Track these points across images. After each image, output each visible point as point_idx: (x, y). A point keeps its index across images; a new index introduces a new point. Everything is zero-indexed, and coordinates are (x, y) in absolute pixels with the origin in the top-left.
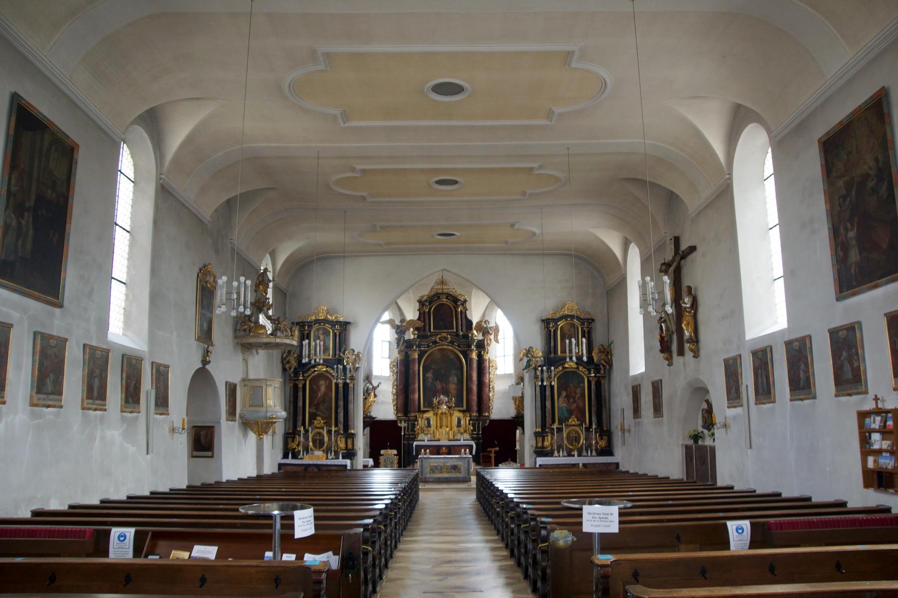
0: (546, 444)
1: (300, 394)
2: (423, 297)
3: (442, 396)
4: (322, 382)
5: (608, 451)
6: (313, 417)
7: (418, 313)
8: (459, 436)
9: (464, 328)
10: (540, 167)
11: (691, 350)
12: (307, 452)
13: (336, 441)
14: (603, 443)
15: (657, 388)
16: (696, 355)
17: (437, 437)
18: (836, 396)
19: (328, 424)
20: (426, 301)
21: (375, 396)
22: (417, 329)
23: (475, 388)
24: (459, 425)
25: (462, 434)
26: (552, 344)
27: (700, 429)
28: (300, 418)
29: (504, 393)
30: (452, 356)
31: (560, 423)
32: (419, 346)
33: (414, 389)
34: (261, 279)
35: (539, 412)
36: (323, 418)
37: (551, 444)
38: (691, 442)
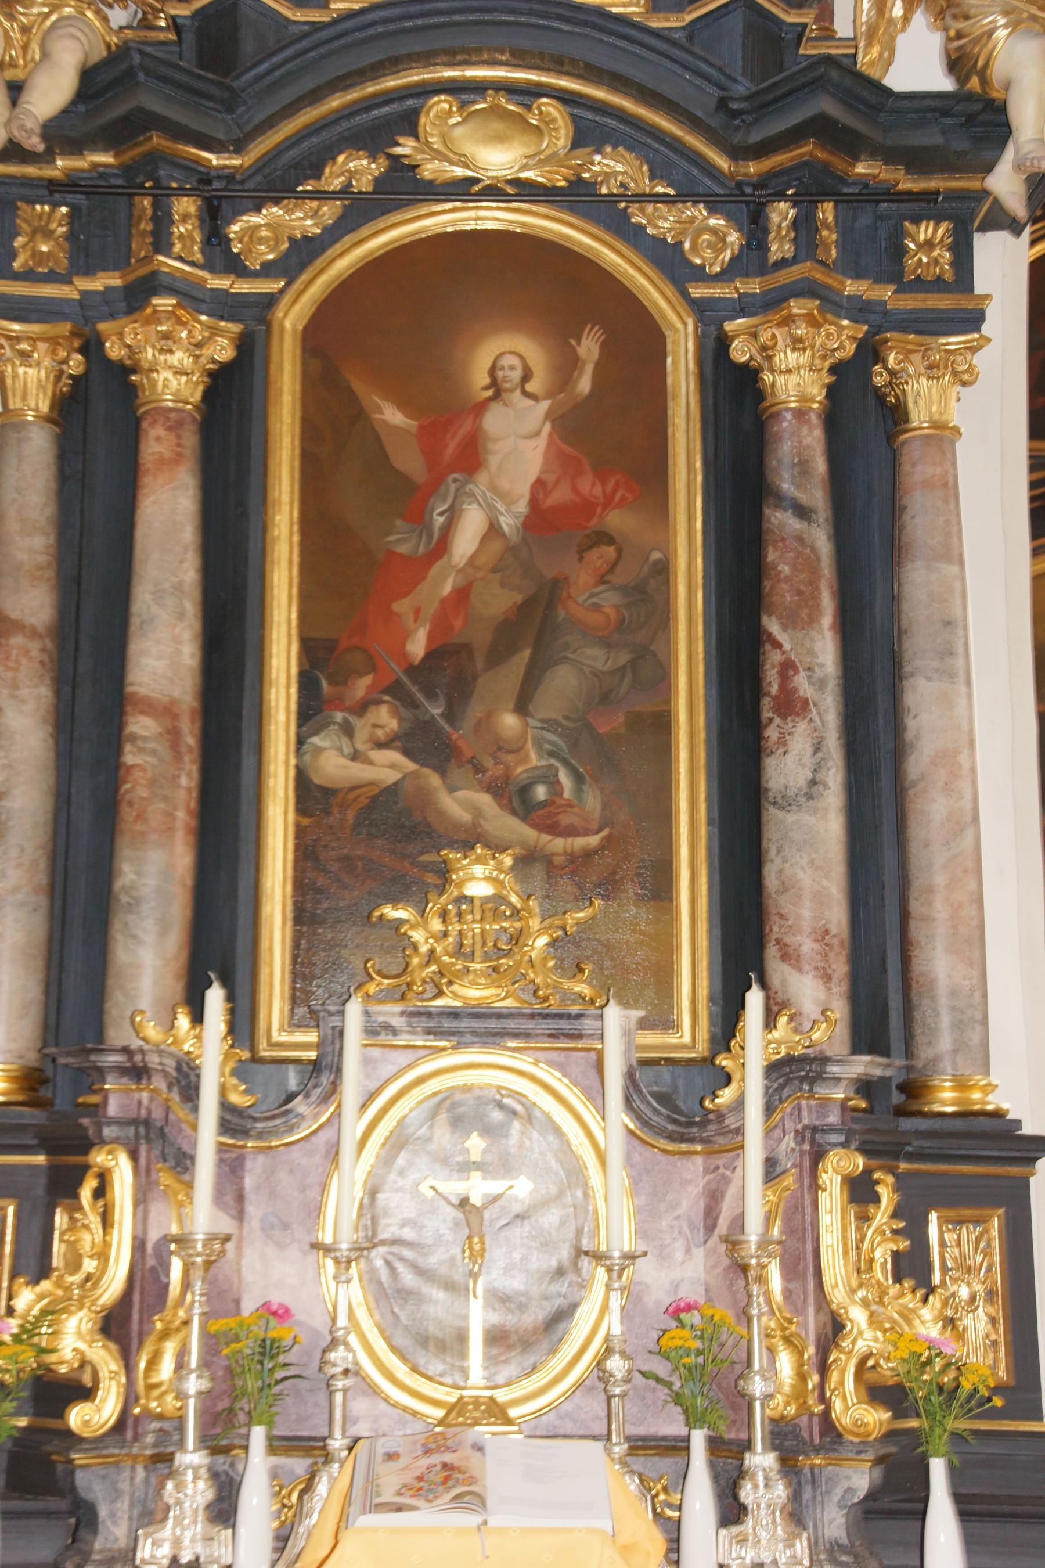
1: (169, 511)
4: (504, 352)
6: (373, 850)
28: (155, 875)
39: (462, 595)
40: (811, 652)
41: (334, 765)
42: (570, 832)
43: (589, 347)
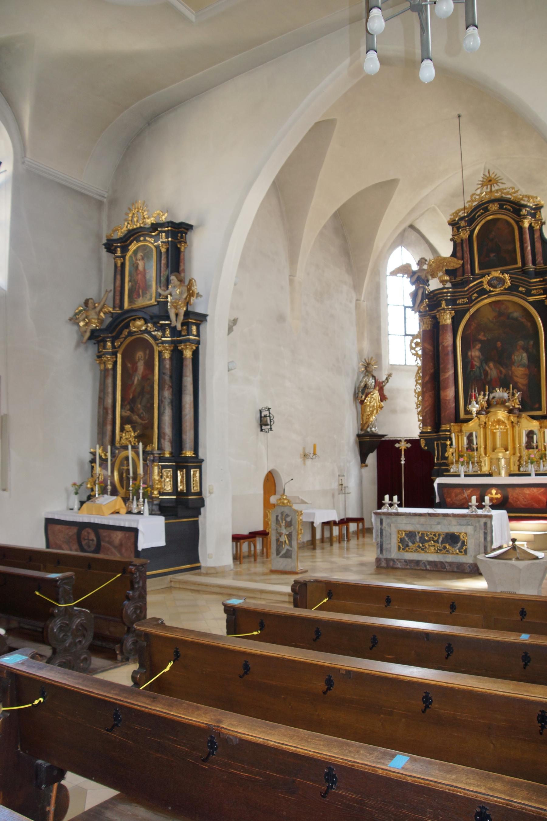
2: (457, 213)
7: (451, 245)
8: (532, 469)
17: (485, 469)
20: (461, 219)
21: (383, 398)
22: (448, 272)
32: (453, 302)
39: (135, 389)
41: (124, 414)
42: (144, 420)
43: (147, 352)
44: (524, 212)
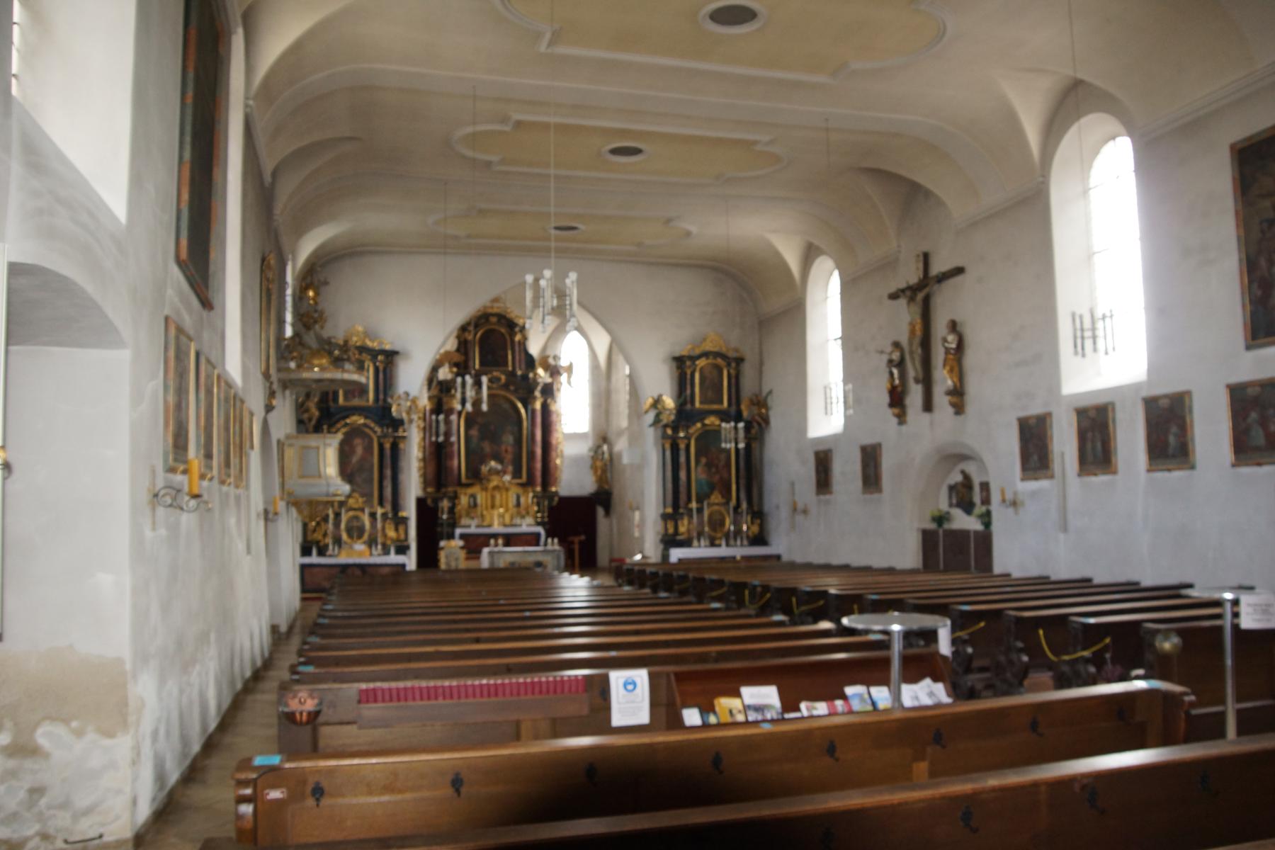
0: (682, 529)
3: (493, 463)
5: (760, 539)
8: (518, 521)
9: (523, 366)
10: (771, 142)
11: (953, 405)
12: (340, 546)
13: (383, 529)
14: (755, 529)
15: (871, 457)
16: (959, 408)
18: (1234, 465)
19: (369, 501)
22: (456, 365)
23: (539, 451)
24: (518, 504)
25: (523, 517)
26: (688, 392)
27: (944, 505)
29: (577, 460)
30: (506, 406)
31: (700, 501)
33: (452, 452)
34: (309, 280)
35: (669, 485)
36: (362, 495)
37: (689, 531)
38: (933, 526)
40: (388, 472)
44: (517, 329)
